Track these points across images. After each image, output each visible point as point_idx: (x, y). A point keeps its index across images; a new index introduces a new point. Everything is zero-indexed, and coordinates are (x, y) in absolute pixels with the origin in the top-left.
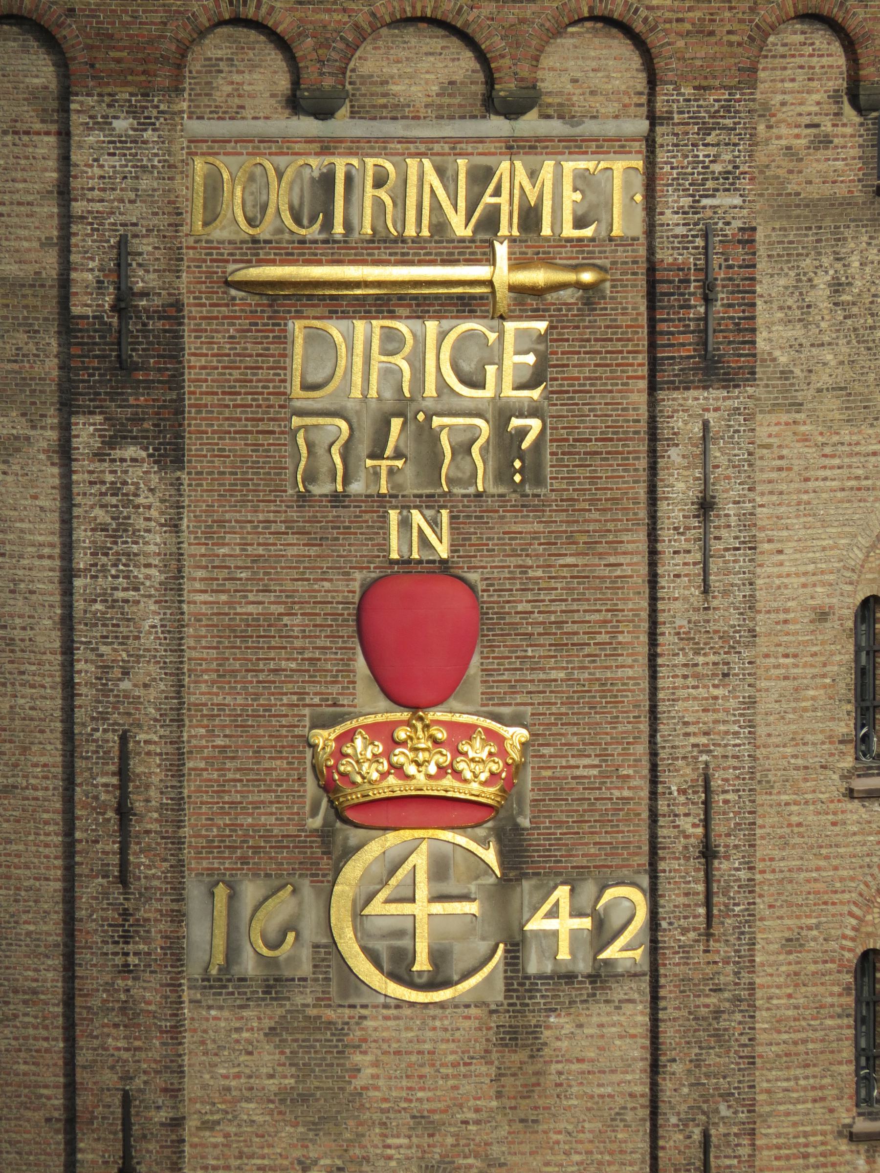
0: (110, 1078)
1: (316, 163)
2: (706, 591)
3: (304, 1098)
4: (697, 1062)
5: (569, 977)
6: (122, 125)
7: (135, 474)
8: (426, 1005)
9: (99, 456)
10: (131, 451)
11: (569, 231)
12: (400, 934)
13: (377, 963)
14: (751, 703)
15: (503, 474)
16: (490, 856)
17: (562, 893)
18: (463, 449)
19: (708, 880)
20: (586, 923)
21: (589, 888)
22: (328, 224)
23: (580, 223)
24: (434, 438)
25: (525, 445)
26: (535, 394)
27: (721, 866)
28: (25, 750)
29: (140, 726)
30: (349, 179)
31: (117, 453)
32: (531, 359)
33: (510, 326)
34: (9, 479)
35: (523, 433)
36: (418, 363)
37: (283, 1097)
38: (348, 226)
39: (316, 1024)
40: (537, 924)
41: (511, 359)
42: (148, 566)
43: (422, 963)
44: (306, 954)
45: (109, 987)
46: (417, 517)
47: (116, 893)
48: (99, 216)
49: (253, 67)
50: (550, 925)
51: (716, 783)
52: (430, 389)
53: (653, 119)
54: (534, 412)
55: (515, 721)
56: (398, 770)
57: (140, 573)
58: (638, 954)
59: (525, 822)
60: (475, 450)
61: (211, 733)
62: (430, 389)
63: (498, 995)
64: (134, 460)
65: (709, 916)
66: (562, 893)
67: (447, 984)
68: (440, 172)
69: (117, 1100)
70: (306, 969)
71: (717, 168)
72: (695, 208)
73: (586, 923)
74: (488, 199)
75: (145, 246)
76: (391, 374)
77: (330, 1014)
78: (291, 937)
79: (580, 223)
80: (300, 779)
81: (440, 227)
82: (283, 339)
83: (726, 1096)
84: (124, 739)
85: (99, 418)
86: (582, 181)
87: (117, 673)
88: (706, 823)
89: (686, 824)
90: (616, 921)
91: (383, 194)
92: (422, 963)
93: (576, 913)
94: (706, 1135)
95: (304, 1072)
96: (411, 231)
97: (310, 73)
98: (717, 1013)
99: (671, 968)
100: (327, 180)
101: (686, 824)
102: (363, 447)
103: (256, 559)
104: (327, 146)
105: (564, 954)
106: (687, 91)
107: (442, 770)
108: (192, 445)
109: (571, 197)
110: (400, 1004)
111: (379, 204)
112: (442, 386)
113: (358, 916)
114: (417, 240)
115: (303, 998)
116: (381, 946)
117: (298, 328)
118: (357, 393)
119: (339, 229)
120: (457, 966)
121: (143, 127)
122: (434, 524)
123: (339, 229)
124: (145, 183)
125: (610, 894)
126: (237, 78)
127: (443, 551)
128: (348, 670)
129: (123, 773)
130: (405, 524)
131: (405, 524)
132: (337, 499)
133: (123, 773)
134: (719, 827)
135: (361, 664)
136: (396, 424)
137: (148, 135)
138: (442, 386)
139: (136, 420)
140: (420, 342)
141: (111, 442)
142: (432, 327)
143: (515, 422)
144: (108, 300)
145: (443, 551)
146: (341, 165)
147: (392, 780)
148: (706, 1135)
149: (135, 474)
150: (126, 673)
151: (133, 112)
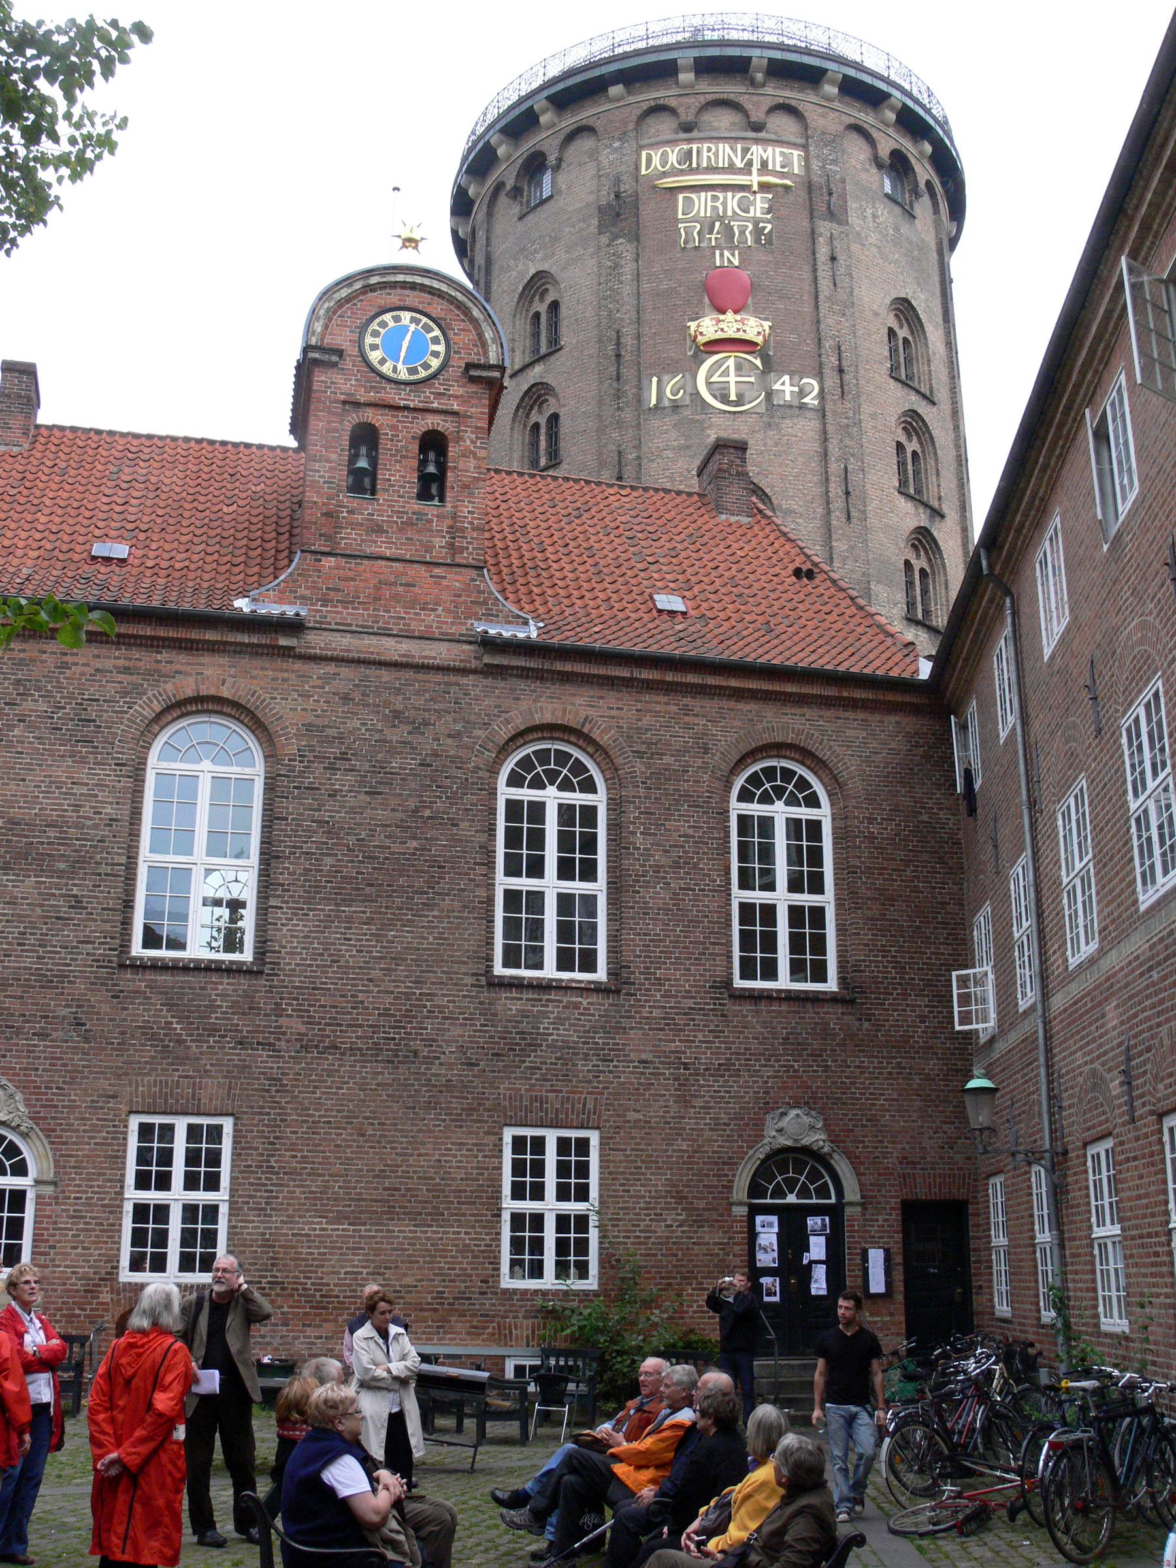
0: (614, 448)
2: (835, 285)
3: (688, 447)
4: (841, 441)
5: (791, 407)
7: (621, 248)
8: (735, 413)
10: (621, 240)
11: (778, 169)
12: (724, 389)
13: (715, 397)
14: (854, 326)
15: (757, 240)
16: (758, 362)
17: (786, 378)
18: (742, 233)
19: (841, 380)
20: (796, 389)
21: (797, 378)
23: (782, 167)
24: (731, 228)
25: (766, 231)
26: (769, 216)
27: (846, 377)
28: (582, 352)
30: (698, 152)
32: (767, 206)
33: (758, 196)
35: (765, 228)
36: (725, 204)
37: (680, 448)
38: (698, 165)
39: (693, 421)
40: (777, 387)
41: (759, 205)
43: (733, 397)
44: (688, 397)
45: (613, 416)
46: (726, 253)
47: (615, 385)
48: (608, 174)
50: (782, 388)
51: (843, 348)
52: (730, 213)
53: (807, 138)
54: (769, 222)
55: (766, 319)
56: (722, 330)
58: (816, 402)
59: (771, 353)
60: (747, 233)
62: (730, 213)
63: (762, 409)
65: (843, 393)
66: (786, 378)
67: (743, 405)
68: (732, 148)
69: (616, 454)
70: (688, 402)
72: (824, 166)
73: (796, 389)
74: (748, 156)
75: (624, 178)
76: (715, 208)
77: (697, 417)
78: (682, 392)
79: (782, 167)
80: (685, 340)
81: (732, 164)
82: (676, 201)
83: (853, 455)
84: (618, 332)
86: (782, 153)
88: (840, 360)
89: (833, 359)
90: (807, 390)
91: (710, 154)
92: (733, 397)
93: (792, 385)
94: (846, 468)
95: (688, 437)
96: (721, 165)
98: (848, 426)
99: (829, 407)
100: (690, 152)
101: (833, 359)
102: (706, 230)
104: (690, 141)
105: (788, 398)
107: (738, 330)
109: (779, 159)
110: (725, 412)
111: (709, 158)
112: (734, 212)
113: (709, 384)
114: (723, 168)
115: (687, 413)
116: (717, 393)
117: (681, 197)
118: (702, 214)
119: (694, 165)
120: (748, 395)
122: (733, 255)
123: (694, 165)
124: (625, 158)
125: (805, 380)
127: (736, 263)
128: (701, 302)
129: (618, 344)
130: (722, 255)
131: (722, 255)
132: (696, 248)
133: (618, 344)
134: (844, 363)
135: (707, 299)
136: (717, 224)
138: (734, 212)
139: (622, 230)
140: (725, 198)
141: (613, 240)
142: (730, 194)
143: (761, 225)
144: (613, 196)
145: (736, 263)
146: (695, 147)
147: (719, 333)
148: (846, 468)
151: (620, 139)
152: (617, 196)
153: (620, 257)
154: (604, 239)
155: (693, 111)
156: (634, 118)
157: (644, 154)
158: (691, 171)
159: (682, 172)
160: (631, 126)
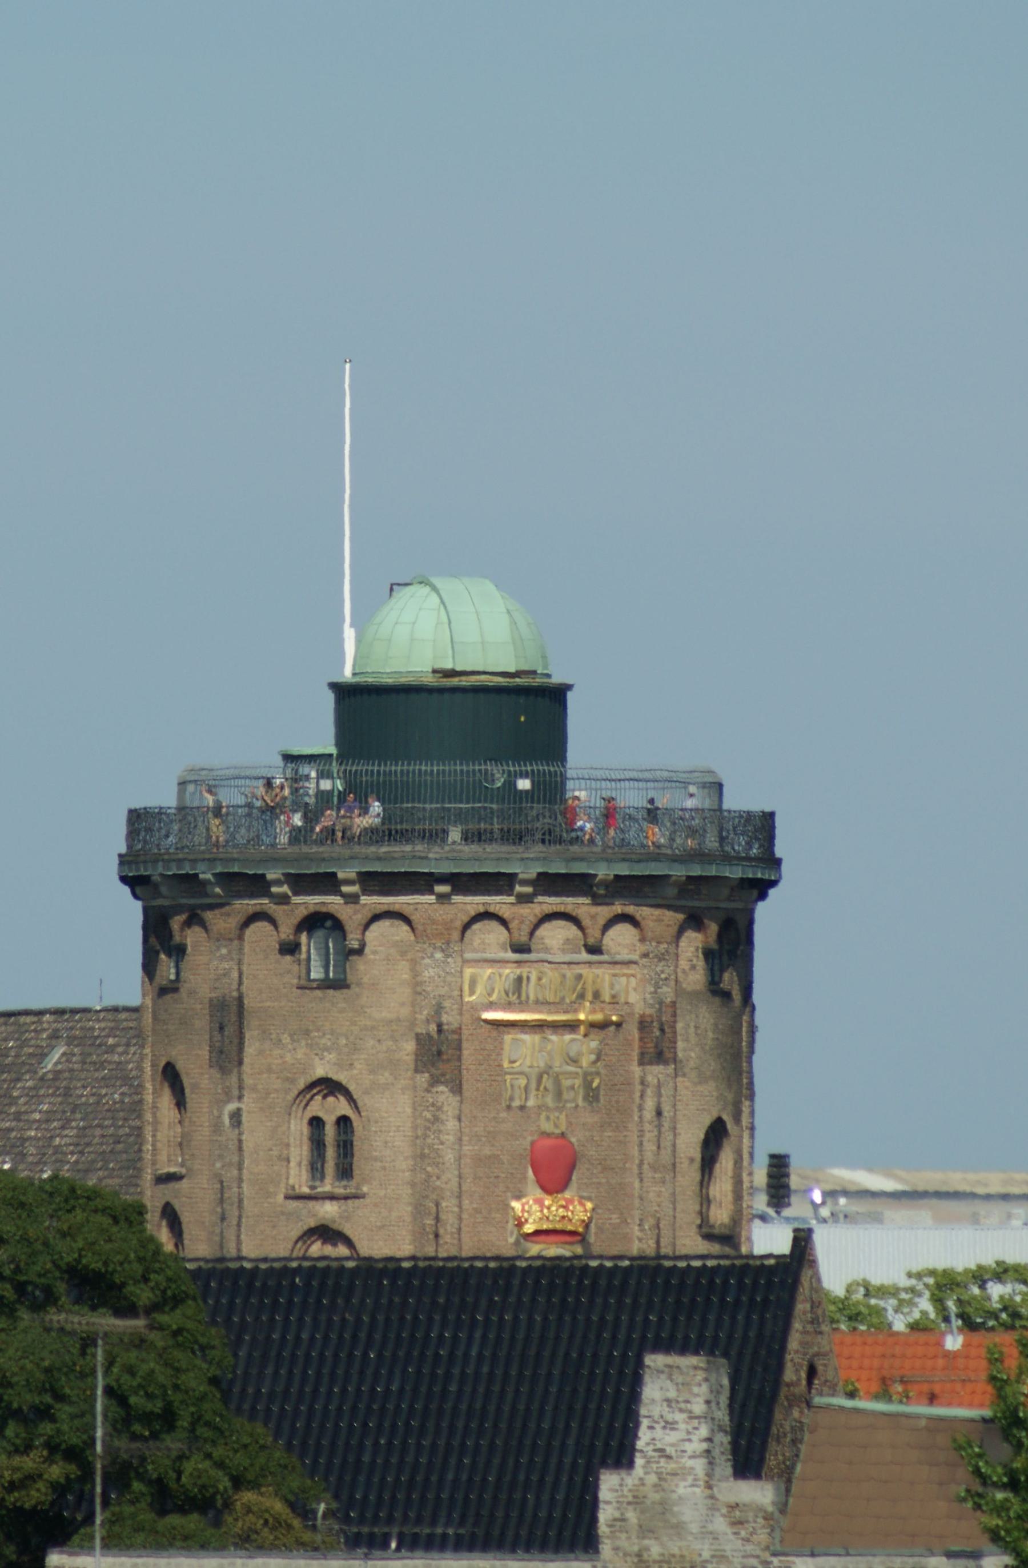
1: (518, 971)
6: (439, 955)
9: (428, 1091)
10: (442, 1088)
22: (519, 997)
29: (443, 1198)
31: (434, 1090)
34: (384, 1100)
42: (448, 1134)
49: (489, 932)
57: (444, 1137)
61: (471, 1203)
64: (442, 1092)
71: (663, 976)
75: (447, 1004)
85: (427, 1075)
87: (435, 1178)
97: (516, 935)
103: (489, 1132)
106: (654, 944)
108: (465, 1087)
117: (508, 1038)
121: (448, 956)
123: (524, 997)
126: (483, 936)
136: (545, 1076)
137: (449, 960)
139: (443, 1075)
144: (433, 1028)
149: (441, 1098)
150: (438, 1178)
151: (443, 951)
152: (440, 1031)
153: (439, 1109)
154: (423, 1079)
155: (526, 929)
156: (459, 924)
157: (468, 972)
158: (522, 1005)
159: (508, 1006)
160: (456, 935)
